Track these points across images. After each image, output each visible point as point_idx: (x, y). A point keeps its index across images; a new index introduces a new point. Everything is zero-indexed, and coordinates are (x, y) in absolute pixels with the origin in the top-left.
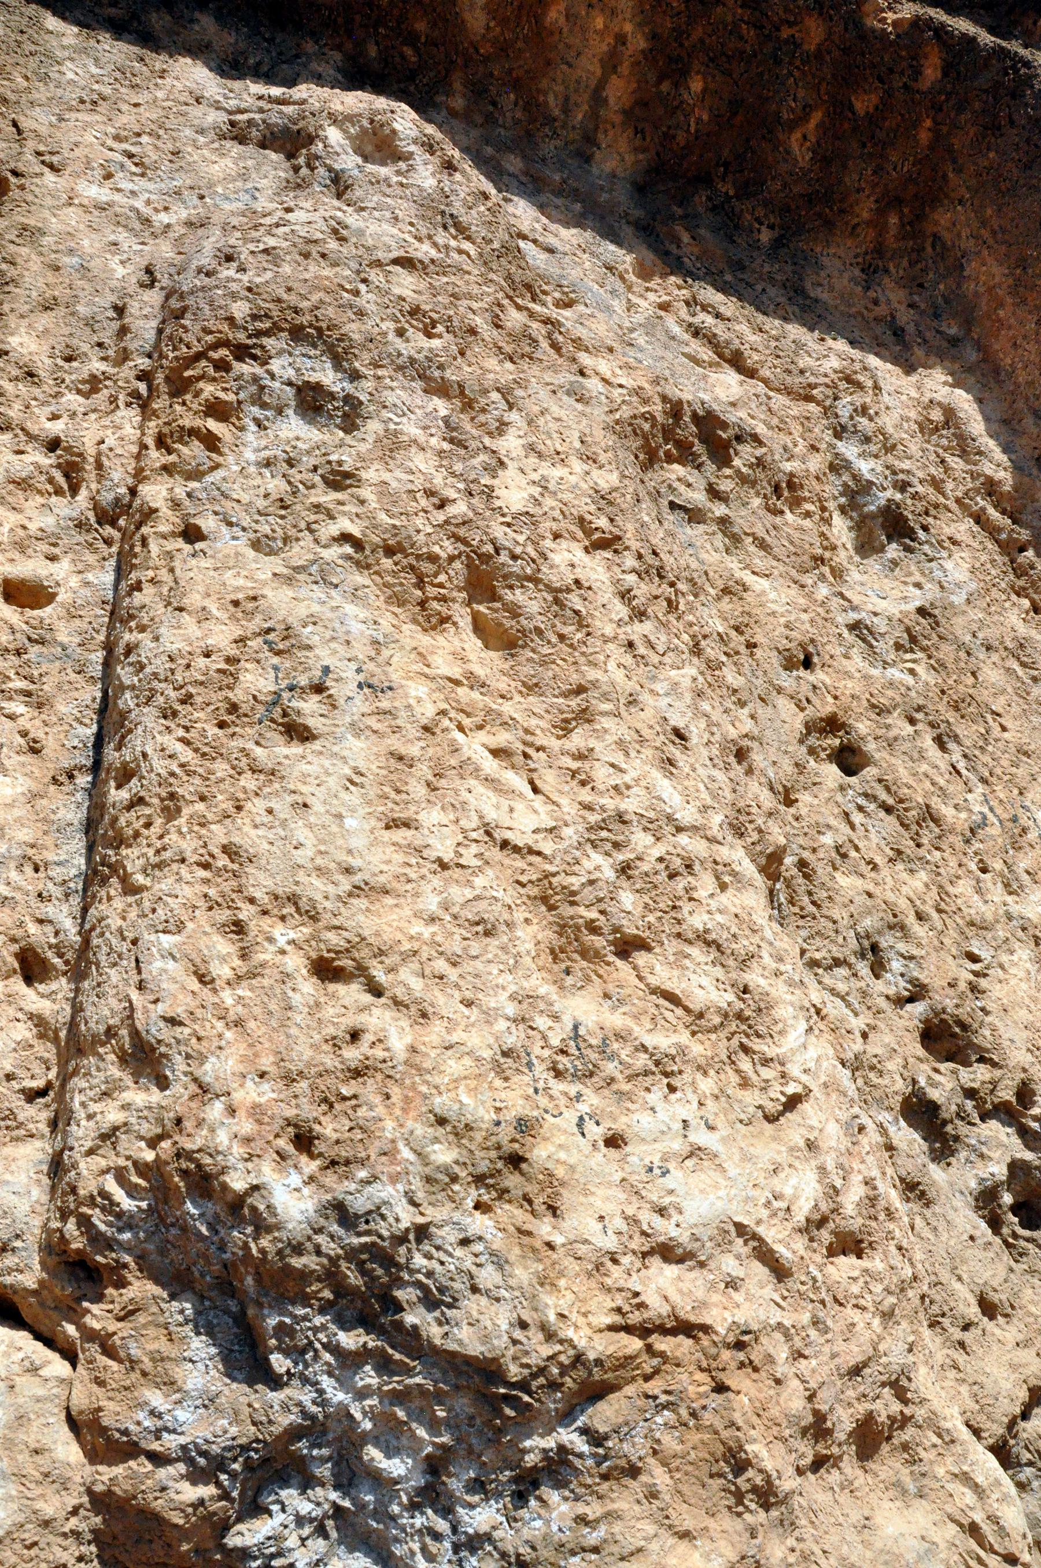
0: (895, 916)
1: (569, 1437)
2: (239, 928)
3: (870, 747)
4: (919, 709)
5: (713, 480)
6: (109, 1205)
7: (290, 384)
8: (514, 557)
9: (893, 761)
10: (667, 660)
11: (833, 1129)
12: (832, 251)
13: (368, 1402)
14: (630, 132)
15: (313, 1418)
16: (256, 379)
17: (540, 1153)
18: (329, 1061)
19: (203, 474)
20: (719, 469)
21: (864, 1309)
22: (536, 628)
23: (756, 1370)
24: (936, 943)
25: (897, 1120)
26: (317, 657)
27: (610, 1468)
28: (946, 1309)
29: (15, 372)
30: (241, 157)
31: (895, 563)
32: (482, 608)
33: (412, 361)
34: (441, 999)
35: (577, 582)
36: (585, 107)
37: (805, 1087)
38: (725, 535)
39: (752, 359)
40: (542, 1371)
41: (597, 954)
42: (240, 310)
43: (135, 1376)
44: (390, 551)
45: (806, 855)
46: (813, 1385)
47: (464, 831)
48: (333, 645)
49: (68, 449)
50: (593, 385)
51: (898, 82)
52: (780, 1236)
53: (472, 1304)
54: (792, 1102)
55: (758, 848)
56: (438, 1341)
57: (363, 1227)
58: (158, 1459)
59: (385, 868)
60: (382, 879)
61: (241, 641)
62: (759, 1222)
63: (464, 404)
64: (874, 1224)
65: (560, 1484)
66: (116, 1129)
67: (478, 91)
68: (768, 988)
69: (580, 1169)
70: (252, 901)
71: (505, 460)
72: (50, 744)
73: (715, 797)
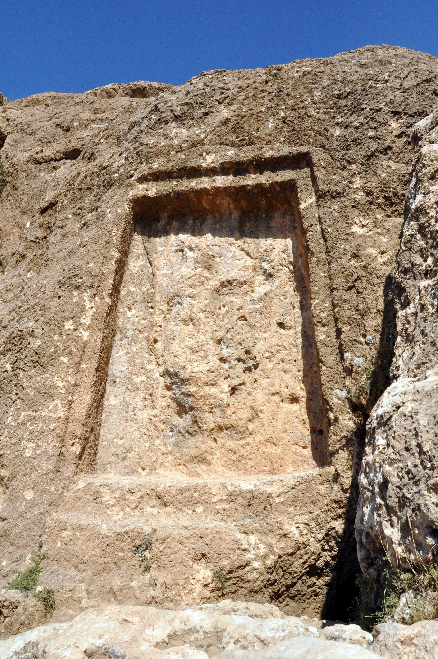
39: (250, 252)
51: (273, 192)
67: (212, 214)
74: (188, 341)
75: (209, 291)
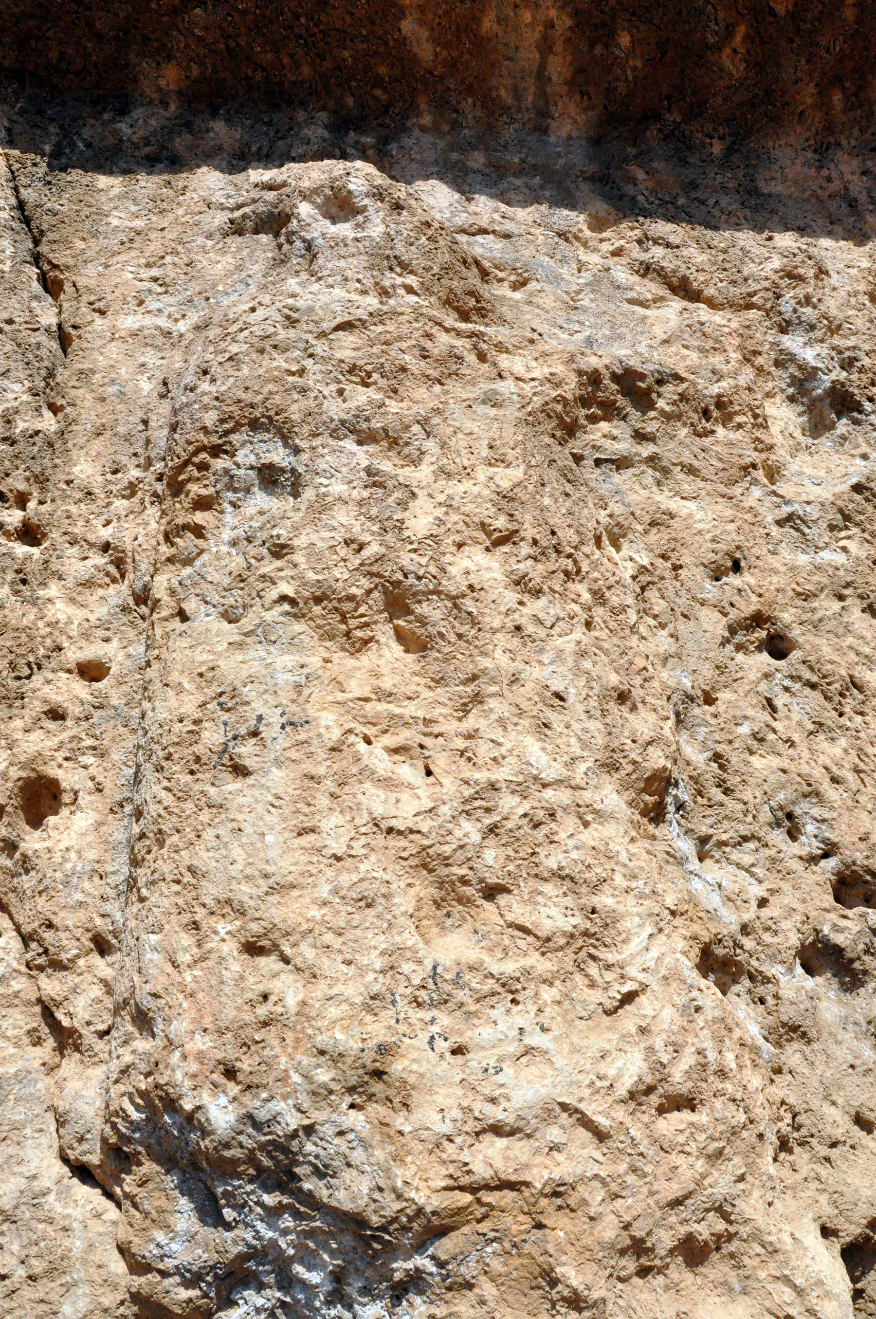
0: (810, 785)
1: (422, 1262)
2: (196, 925)
3: (795, 633)
4: (848, 585)
5: (638, 426)
6: (126, 1118)
7: (252, 468)
8: (419, 578)
9: (817, 641)
10: (557, 630)
11: (668, 1013)
12: (782, 142)
13: (289, 1237)
14: (577, 97)
15: (254, 1247)
16: (226, 471)
17: (397, 1067)
18: (248, 1017)
19: (193, 560)
20: (644, 413)
21: (689, 1154)
22: (439, 633)
23: (572, 1210)
24: (850, 802)
25: (790, 970)
26: (253, 709)
27: (452, 1283)
28: (814, 1131)
29: (79, 495)
30: (239, 250)
31: (844, 438)
32: (401, 622)
33: (343, 422)
34: (325, 963)
35: (471, 587)
36: (532, 90)
37: (641, 983)
38: (655, 469)
39: (697, 280)
40: (395, 1220)
41: (469, 900)
42: (210, 418)
43: (148, 1221)
44: (318, 600)
45: (720, 748)
46: (627, 1218)
47: (356, 827)
48: (266, 696)
49: (115, 549)
50: (507, 387)
52: (600, 1109)
53: (348, 1175)
54: (629, 998)
55: (634, 776)
56: (325, 1200)
57: (266, 1130)
58: (164, 1274)
59: (293, 869)
60: (290, 878)
61: (203, 705)
62: (581, 1100)
63: (390, 444)
64: (704, 1085)
65: (421, 1292)
66: (128, 1067)
67: (441, 105)
68: (615, 906)
69: (428, 1075)
70: (204, 905)
71: (416, 490)
72: (108, 785)
73: (585, 745)
74: (388, 783)
75: (511, 413)
